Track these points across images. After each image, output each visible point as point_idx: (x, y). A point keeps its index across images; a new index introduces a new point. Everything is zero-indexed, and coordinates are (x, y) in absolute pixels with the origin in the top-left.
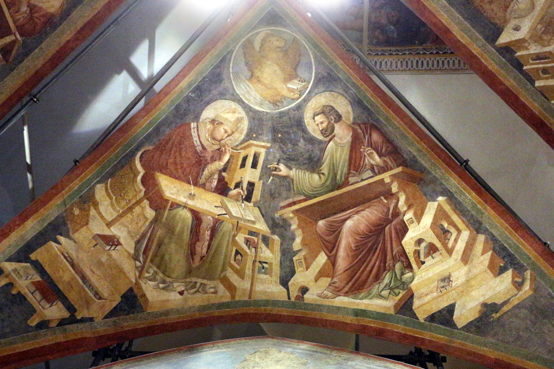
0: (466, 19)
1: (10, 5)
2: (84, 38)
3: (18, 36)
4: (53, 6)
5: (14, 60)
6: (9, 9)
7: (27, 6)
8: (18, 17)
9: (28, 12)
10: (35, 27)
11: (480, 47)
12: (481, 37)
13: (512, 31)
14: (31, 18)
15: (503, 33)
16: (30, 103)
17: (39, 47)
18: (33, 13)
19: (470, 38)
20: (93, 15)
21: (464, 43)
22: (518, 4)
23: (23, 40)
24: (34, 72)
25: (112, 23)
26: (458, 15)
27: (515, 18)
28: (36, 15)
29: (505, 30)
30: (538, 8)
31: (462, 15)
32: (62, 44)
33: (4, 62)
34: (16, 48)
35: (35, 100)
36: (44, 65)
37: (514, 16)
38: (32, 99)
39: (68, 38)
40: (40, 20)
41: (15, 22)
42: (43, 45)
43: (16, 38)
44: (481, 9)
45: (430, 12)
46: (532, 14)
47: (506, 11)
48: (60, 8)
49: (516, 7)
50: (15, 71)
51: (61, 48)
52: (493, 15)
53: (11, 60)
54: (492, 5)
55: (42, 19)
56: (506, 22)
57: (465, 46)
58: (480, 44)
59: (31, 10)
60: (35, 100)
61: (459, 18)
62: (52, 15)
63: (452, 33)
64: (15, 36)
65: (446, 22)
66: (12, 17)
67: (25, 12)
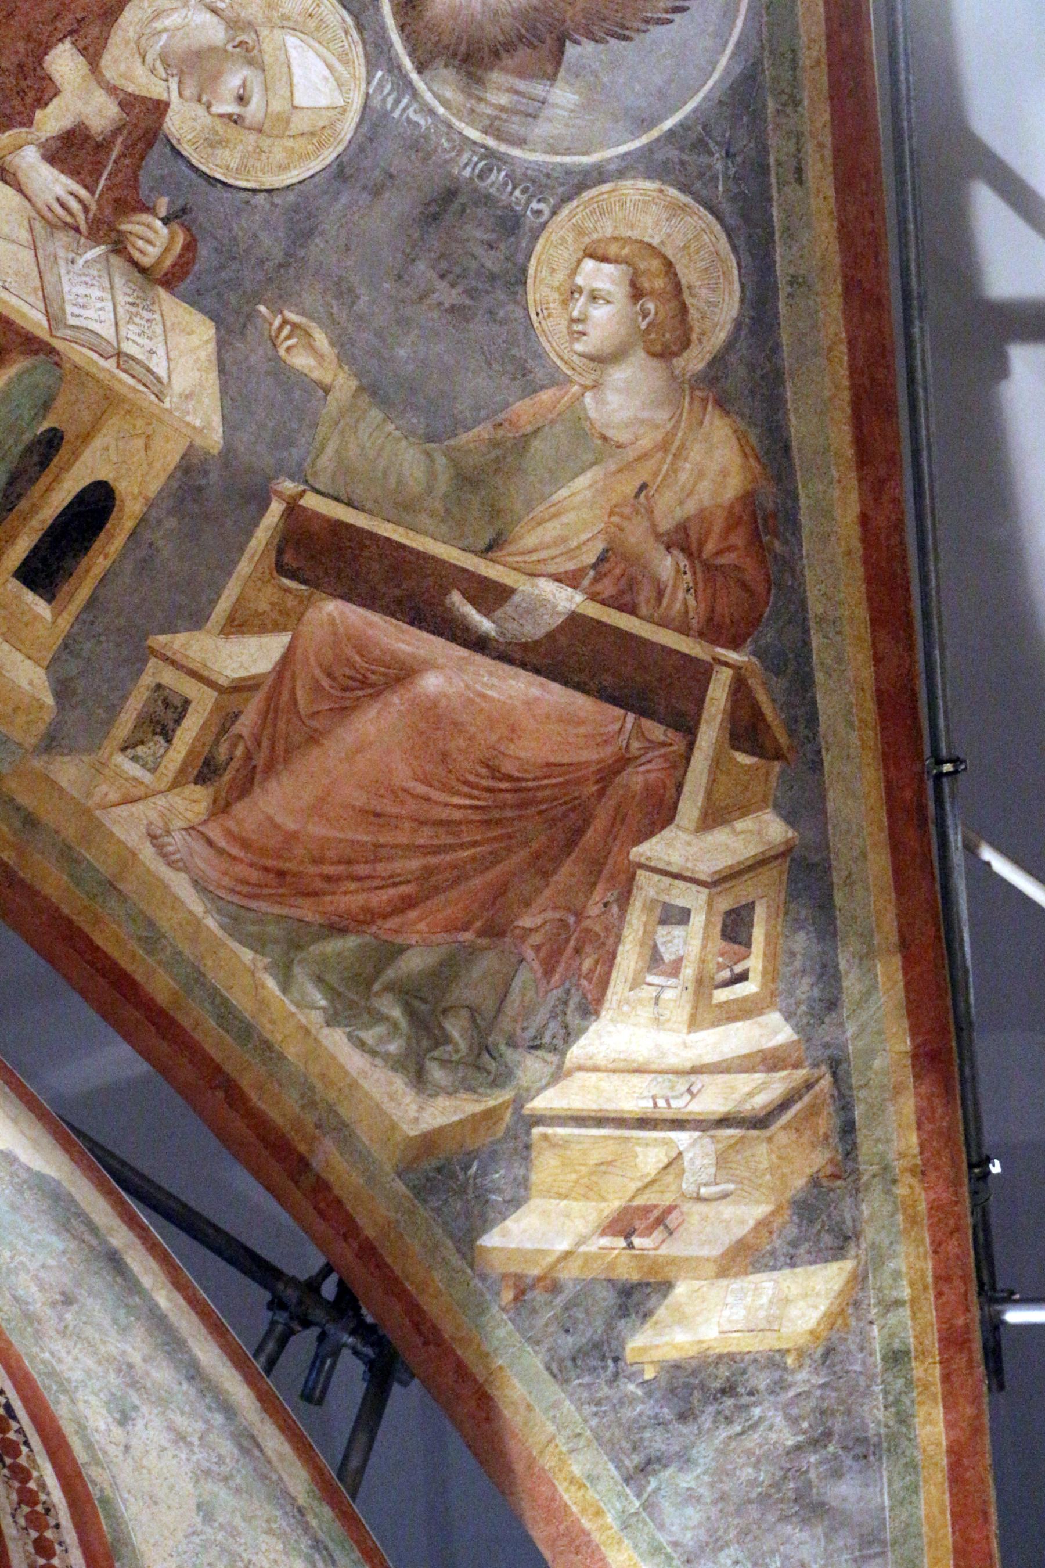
1: (627, 598)
2: (893, 460)
3: (732, 656)
4: (724, 473)
5: (791, 733)
6: (631, 610)
7: (662, 548)
8: (678, 606)
9: (684, 562)
10: (744, 585)
14: (709, 568)
16: (947, 790)
17: (812, 624)
18: (700, 551)
20: (844, 372)
23: (754, 653)
24: (871, 705)
25: (908, 323)
28: (710, 547)
32: (856, 544)
33: (777, 766)
34: (762, 697)
35: (947, 767)
36: (878, 660)
38: (940, 775)
39: (854, 509)
40: (731, 549)
41: (684, 629)
42: (816, 607)
43: (736, 668)
48: (745, 455)
50: (827, 758)
51: (866, 560)
53: (783, 740)
55: (738, 539)
59: (686, 550)
60: (947, 767)
62: (748, 498)
64: (726, 664)
66: (663, 623)
67: (679, 571)
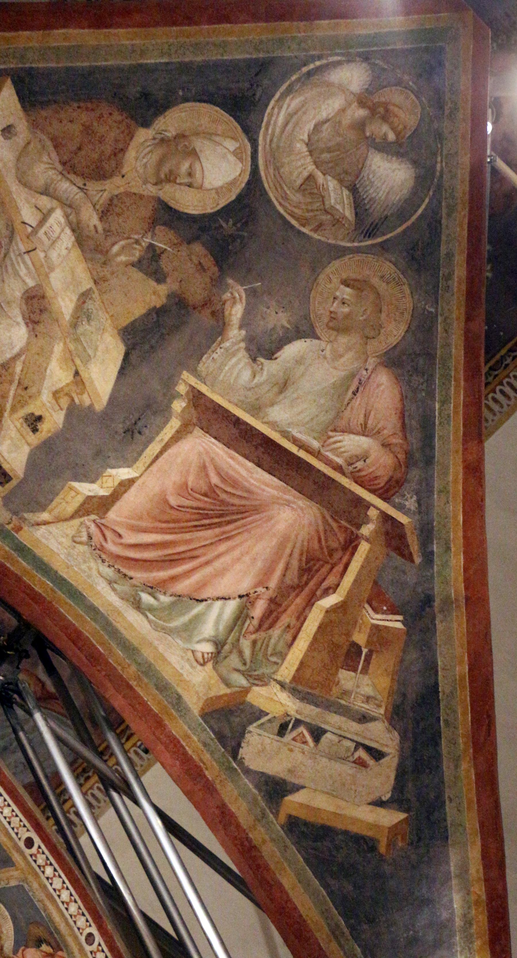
0: (92, 71)
11: (26, 49)
12: (41, 65)
13: (11, 121)
15: (19, 106)
19: (54, 48)
21: (56, 32)
22: (47, 166)
26: (110, 63)
27: (29, 143)
29: (21, 113)
30: (14, 187)
31: (105, 69)
37: (32, 145)
44: (89, 105)
45: (157, 24)
46: (13, 171)
47: (54, 139)
49: (45, 158)
52: (62, 115)
54: (81, 128)
56: (34, 125)
57: (48, 27)
58: (30, 55)
61: (106, 60)
63: (89, 27)
65: (115, 35)
